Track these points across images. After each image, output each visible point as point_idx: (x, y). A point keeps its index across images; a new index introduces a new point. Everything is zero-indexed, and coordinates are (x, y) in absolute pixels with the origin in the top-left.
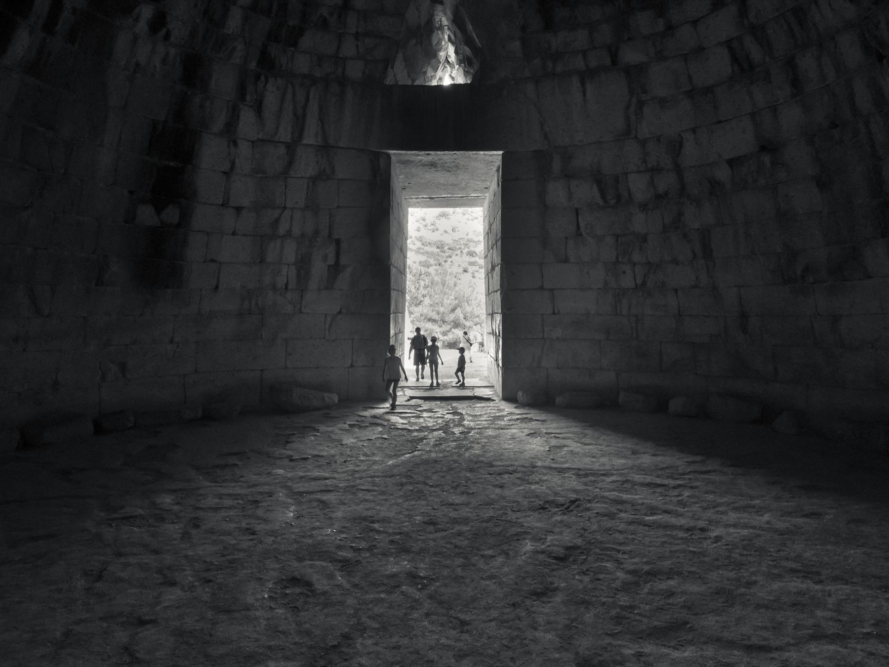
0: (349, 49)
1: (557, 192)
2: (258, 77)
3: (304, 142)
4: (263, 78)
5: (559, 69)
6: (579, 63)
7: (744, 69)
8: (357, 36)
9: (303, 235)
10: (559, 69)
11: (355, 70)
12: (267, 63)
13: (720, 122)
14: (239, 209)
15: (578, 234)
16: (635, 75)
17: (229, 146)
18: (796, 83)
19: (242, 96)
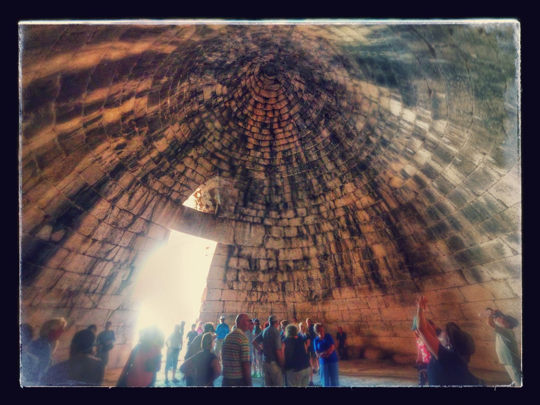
0: (176, 188)
1: (233, 262)
2: (137, 184)
3: (142, 217)
4: (140, 185)
5: (244, 219)
6: (251, 220)
7: (300, 235)
8: (182, 184)
9: (119, 261)
10: (244, 219)
11: (174, 196)
12: (145, 180)
13: (291, 248)
14: (95, 241)
15: (237, 280)
16: (268, 228)
17: (109, 208)
18: (315, 242)
19: (128, 189)
